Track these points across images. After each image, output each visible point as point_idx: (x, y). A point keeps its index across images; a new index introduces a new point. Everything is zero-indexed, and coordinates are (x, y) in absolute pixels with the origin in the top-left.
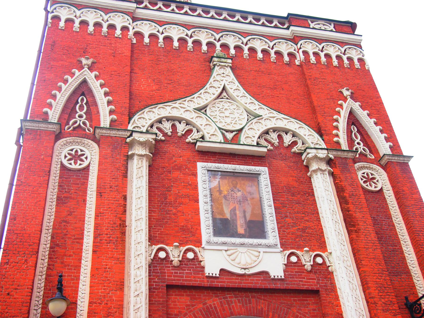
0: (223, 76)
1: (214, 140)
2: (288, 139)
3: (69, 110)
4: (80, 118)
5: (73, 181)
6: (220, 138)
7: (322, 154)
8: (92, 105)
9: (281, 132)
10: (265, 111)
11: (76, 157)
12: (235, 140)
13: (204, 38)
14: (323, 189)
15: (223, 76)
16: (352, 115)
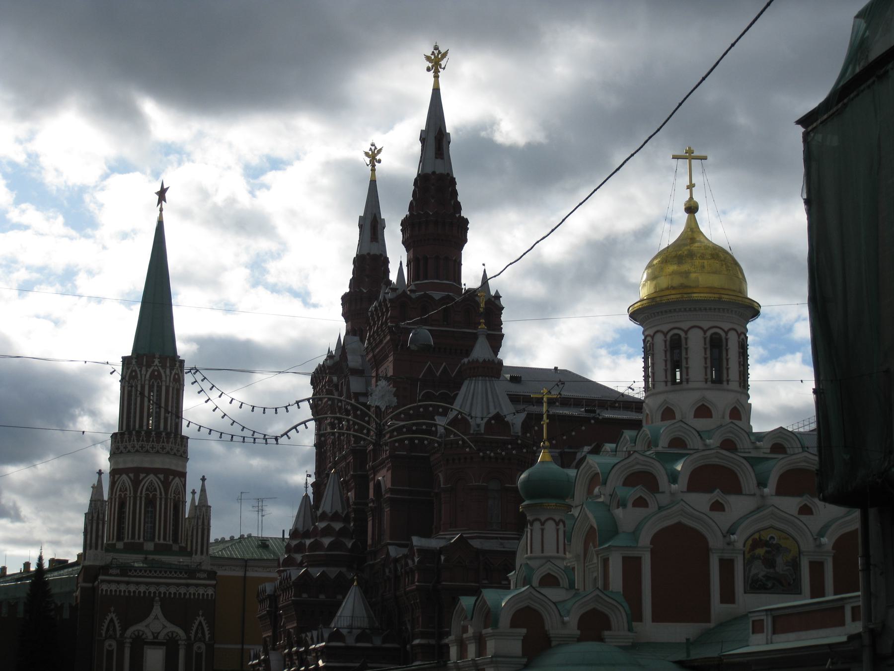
0: (157, 610)
1: (150, 637)
2: (175, 635)
3: (108, 630)
4: (111, 632)
5: (110, 653)
6: (152, 637)
7: (183, 643)
8: (114, 626)
9: (172, 633)
10: (168, 624)
11: (110, 646)
12: (156, 638)
13: (152, 590)
14: (182, 653)
15: (157, 610)
16: (200, 623)
